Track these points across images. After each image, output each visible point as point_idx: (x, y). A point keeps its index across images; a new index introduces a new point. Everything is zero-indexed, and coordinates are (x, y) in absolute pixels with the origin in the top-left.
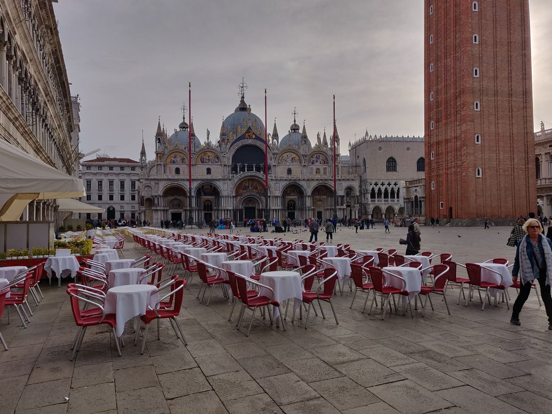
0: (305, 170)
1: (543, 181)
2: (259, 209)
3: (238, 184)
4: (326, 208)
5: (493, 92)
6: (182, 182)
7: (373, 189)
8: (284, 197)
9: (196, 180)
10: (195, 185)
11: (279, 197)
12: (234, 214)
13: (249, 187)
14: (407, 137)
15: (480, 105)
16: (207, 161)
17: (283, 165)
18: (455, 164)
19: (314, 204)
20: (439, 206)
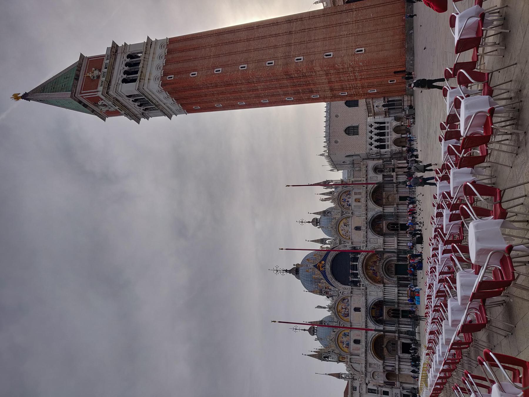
0: (356, 213)
2: (397, 260)
3: (370, 281)
4: (395, 192)
6: (368, 338)
7: (376, 147)
8: (384, 235)
9: (366, 323)
10: (371, 325)
11: (384, 239)
13: (374, 270)
14: (325, 118)
17: (352, 235)
18: (351, 73)
19: (392, 204)
20: (393, 83)
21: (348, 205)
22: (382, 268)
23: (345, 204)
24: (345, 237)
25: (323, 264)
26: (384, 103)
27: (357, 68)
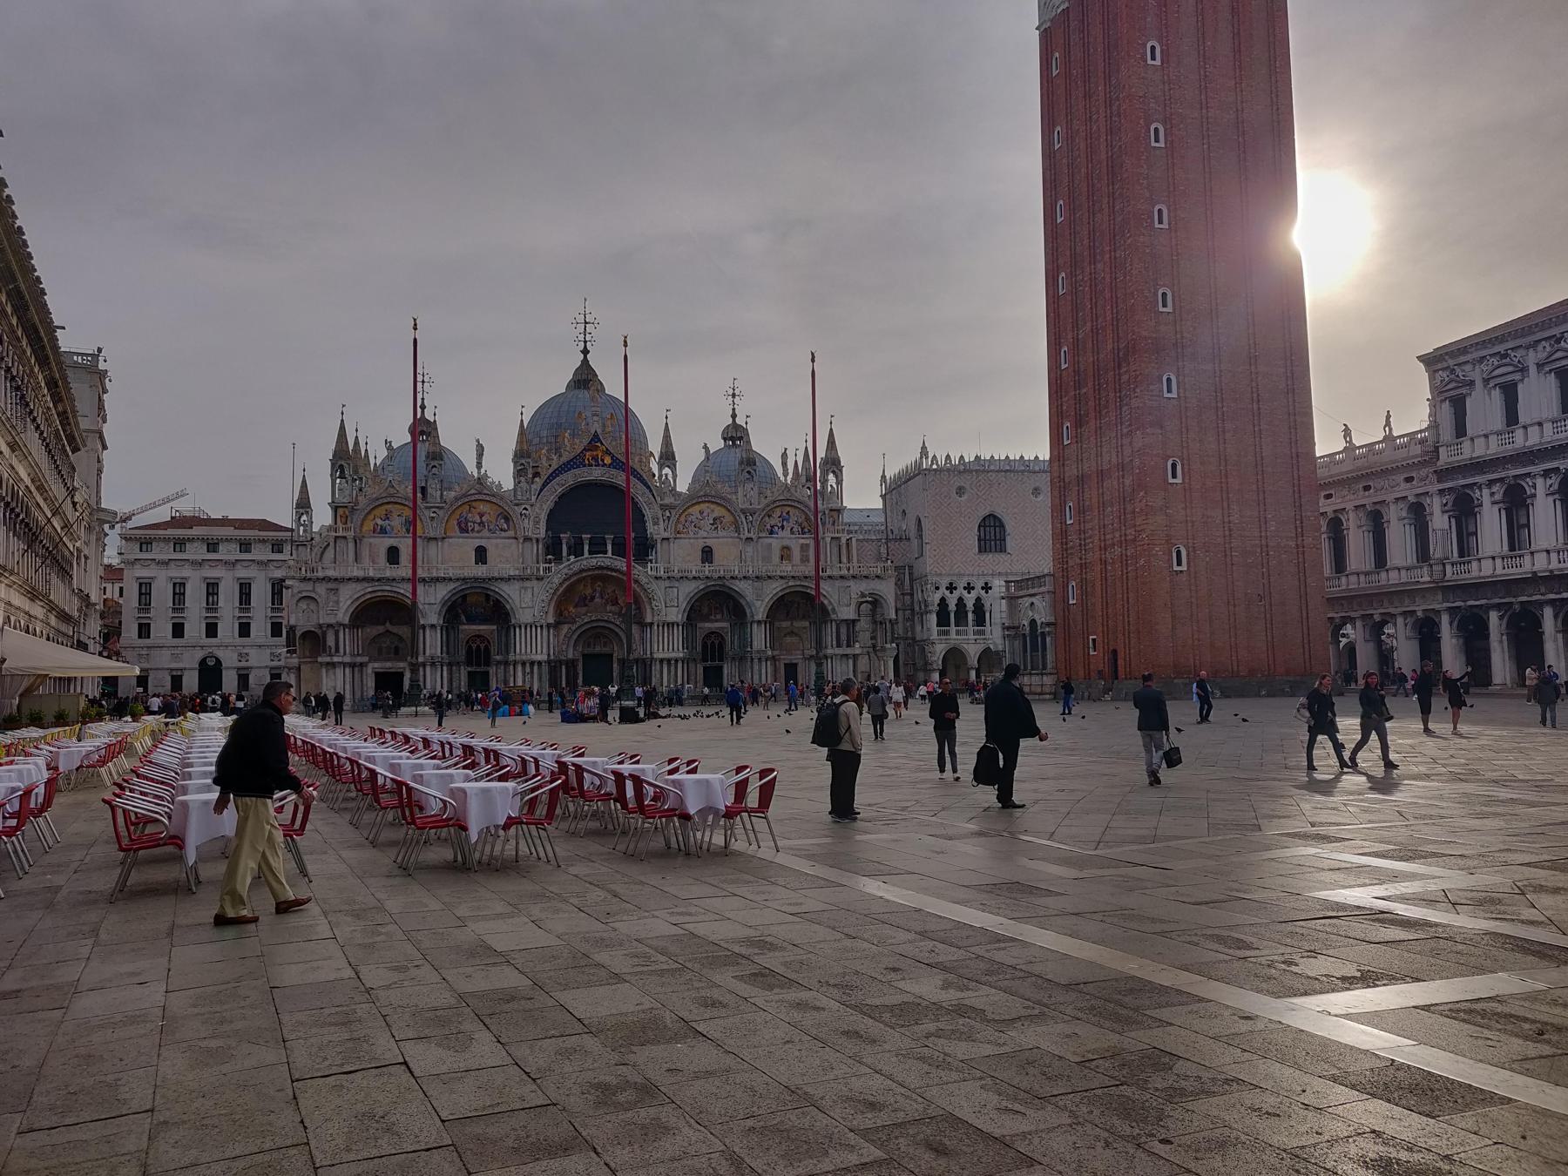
0: (749, 549)
1: (1353, 579)
3: (561, 589)
5: (1211, 351)
9: (444, 579)
11: (678, 625)
12: (550, 673)
13: (593, 598)
14: (1032, 458)
15: (1178, 383)
16: (477, 528)
21: (772, 527)
22: (600, 620)
23: (775, 520)
24: (682, 519)
25: (603, 460)
26: (1039, 623)
27: (1133, 551)
